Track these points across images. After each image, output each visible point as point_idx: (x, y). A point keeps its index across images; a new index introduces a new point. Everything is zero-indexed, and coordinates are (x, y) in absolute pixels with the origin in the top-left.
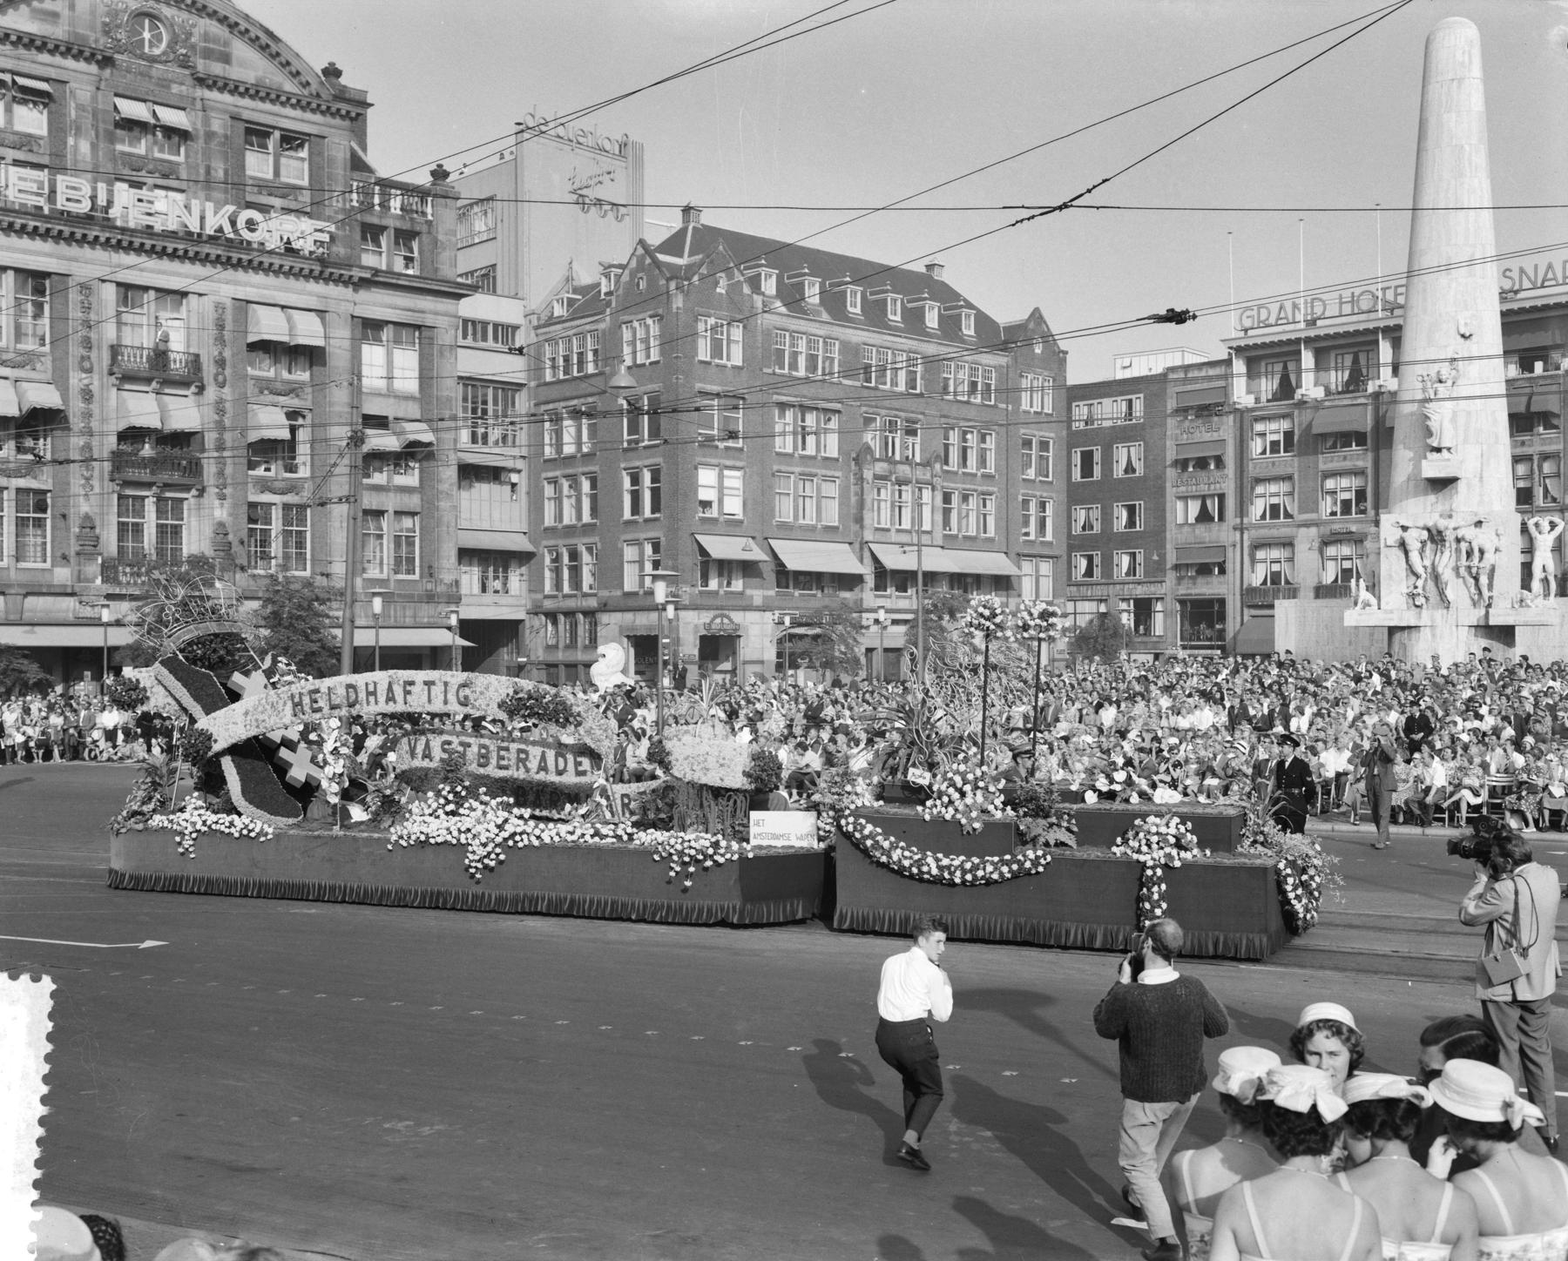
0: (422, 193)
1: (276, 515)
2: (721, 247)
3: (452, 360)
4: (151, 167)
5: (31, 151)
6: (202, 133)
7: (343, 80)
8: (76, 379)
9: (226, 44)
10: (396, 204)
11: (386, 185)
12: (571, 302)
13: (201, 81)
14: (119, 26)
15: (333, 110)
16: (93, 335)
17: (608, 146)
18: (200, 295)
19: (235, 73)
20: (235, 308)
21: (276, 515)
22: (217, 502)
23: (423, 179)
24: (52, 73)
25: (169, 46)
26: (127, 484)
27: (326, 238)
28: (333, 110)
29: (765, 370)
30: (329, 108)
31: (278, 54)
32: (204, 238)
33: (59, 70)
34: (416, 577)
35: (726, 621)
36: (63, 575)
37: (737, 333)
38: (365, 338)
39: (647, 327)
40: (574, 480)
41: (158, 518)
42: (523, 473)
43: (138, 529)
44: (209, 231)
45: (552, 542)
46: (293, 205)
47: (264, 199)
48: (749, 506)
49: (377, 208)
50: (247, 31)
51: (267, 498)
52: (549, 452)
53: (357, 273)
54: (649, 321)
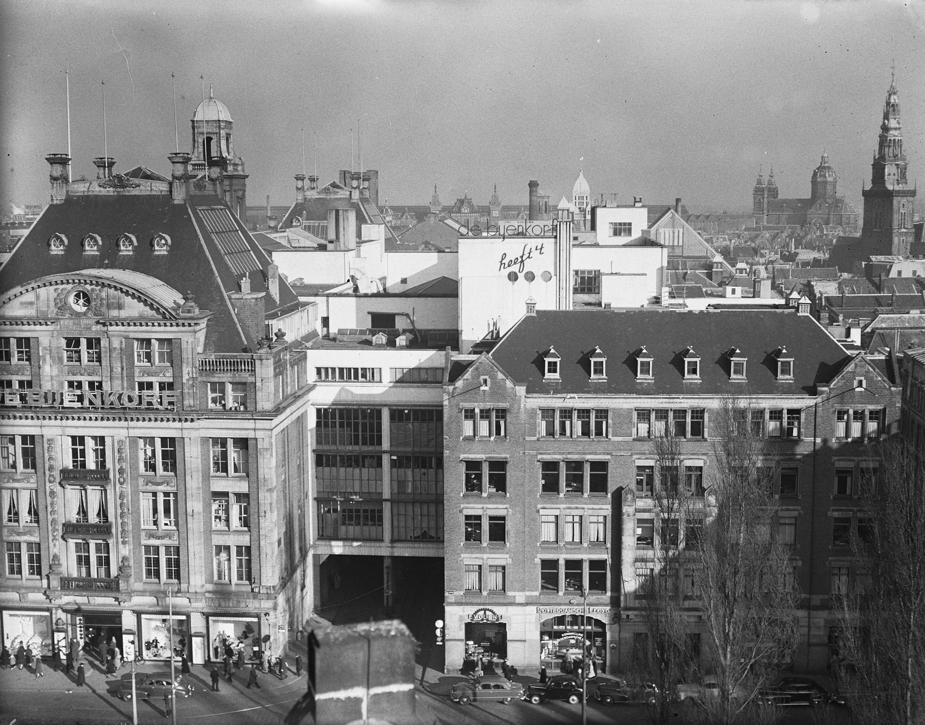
19: (123, 314)
21: (162, 551)
29: (528, 438)
35: (488, 612)
51: (153, 542)
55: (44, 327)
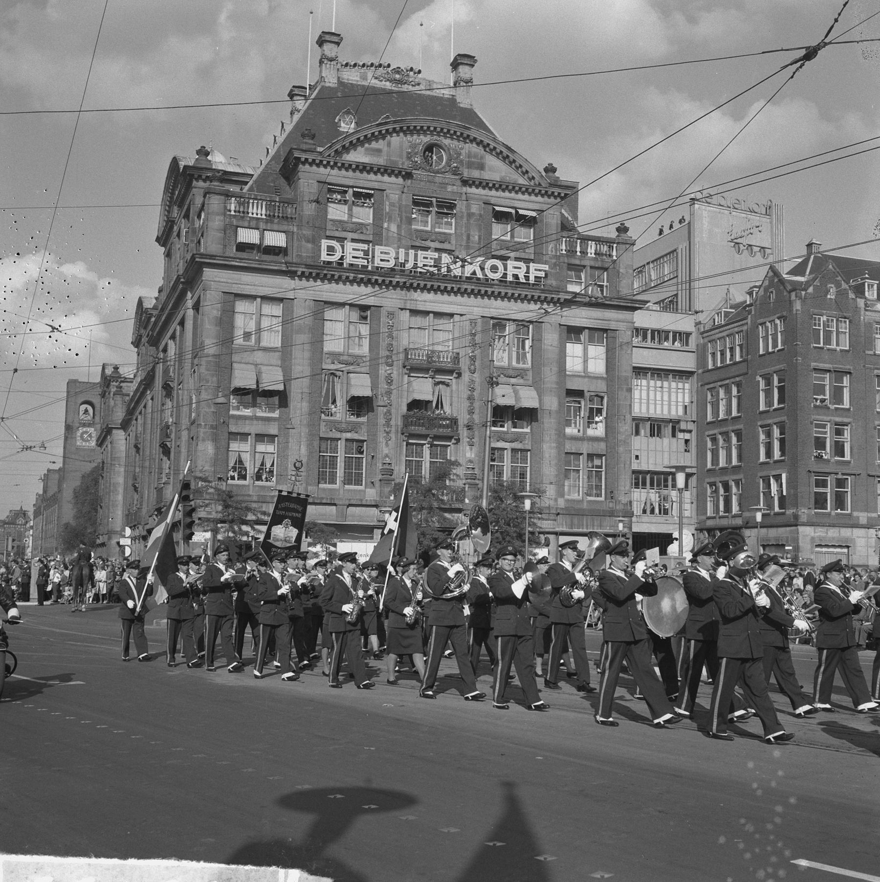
0: (609, 242)
1: (507, 455)
2: (831, 267)
3: (629, 352)
4: (433, 237)
5: (362, 233)
6: (465, 214)
7: (557, 174)
8: (383, 370)
9: (482, 158)
10: (591, 249)
11: (585, 239)
12: (727, 314)
13: (465, 183)
14: (416, 154)
15: (550, 193)
16: (394, 343)
17: (756, 208)
18: (461, 315)
19: (487, 175)
20: (483, 322)
21: (507, 455)
22: (468, 448)
23: (611, 233)
24: (376, 185)
25: (447, 163)
26: (412, 436)
27: (542, 274)
28: (550, 193)
30: (546, 192)
31: (514, 161)
32: (464, 279)
33: (380, 184)
34: (602, 499)
36: (371, 494)
37: (845, 327)
38: (569, 339)
39: (776, 325)
40: (726, 435)
41: (430, 458)
42: (693, 433)
43: (419, 464)
44: (467, 274)
45: (712, 480)
46: (523, 255)
47: (503, 252)
48: (855, 450)
49: (578, 254)
50: (495, 148)
51: (500, 444)
52: (709, 418)
53: (563, 296)
54: (778, 322)
55: (393, 179)
